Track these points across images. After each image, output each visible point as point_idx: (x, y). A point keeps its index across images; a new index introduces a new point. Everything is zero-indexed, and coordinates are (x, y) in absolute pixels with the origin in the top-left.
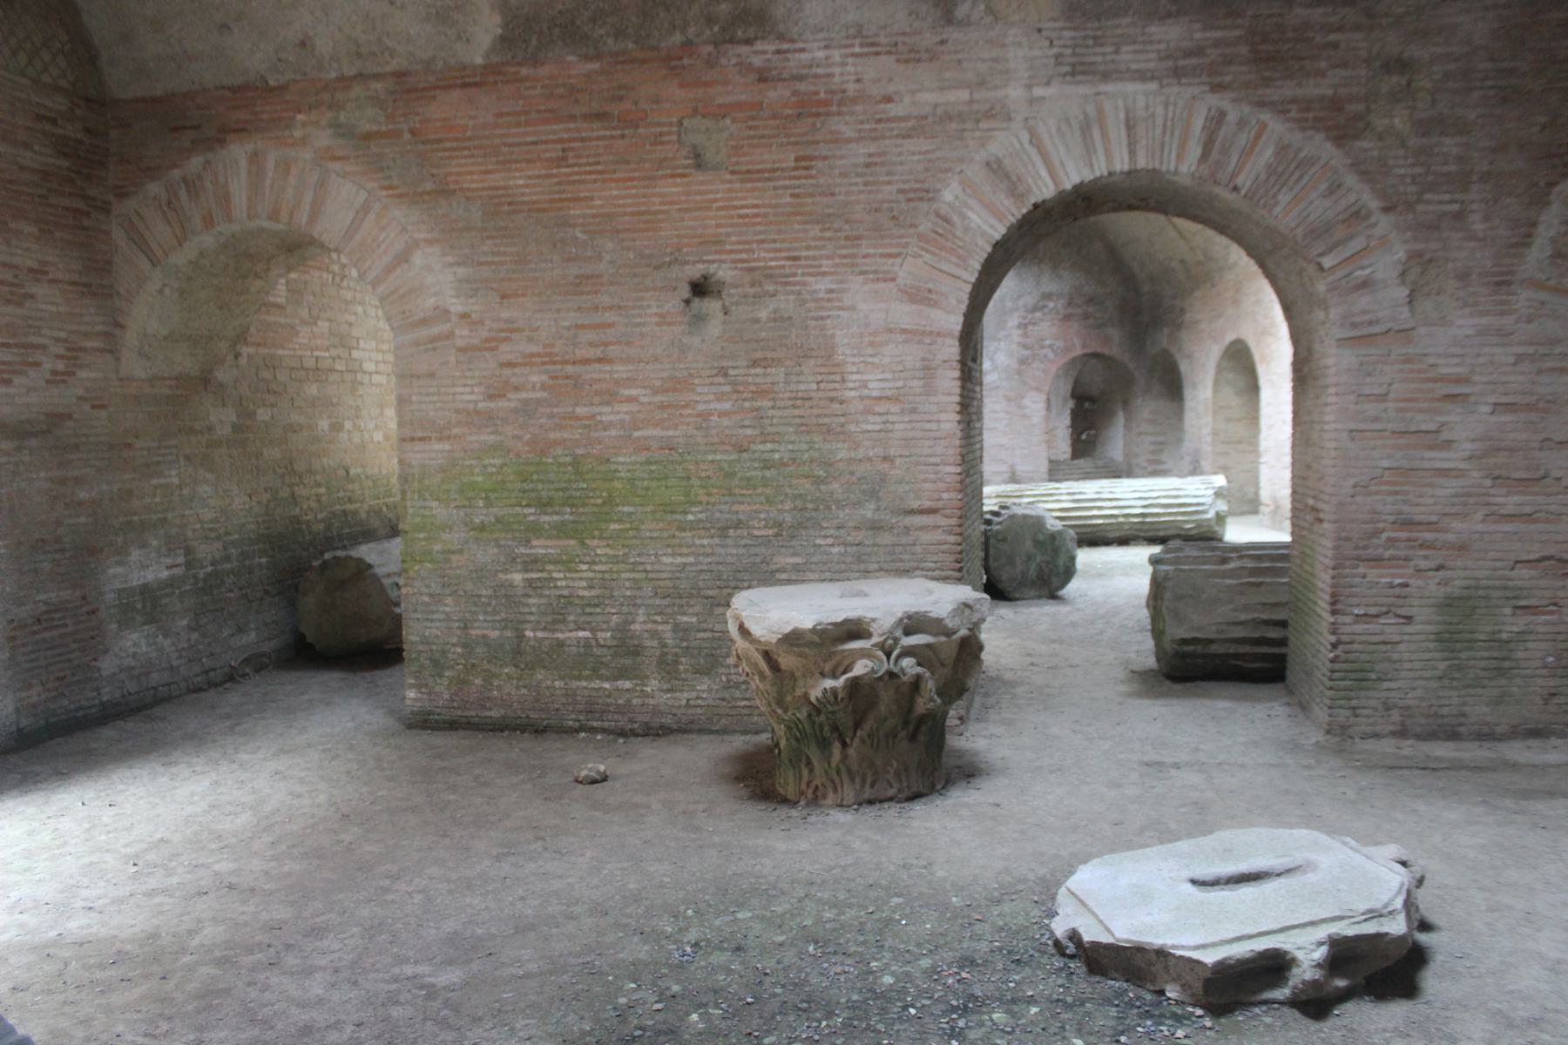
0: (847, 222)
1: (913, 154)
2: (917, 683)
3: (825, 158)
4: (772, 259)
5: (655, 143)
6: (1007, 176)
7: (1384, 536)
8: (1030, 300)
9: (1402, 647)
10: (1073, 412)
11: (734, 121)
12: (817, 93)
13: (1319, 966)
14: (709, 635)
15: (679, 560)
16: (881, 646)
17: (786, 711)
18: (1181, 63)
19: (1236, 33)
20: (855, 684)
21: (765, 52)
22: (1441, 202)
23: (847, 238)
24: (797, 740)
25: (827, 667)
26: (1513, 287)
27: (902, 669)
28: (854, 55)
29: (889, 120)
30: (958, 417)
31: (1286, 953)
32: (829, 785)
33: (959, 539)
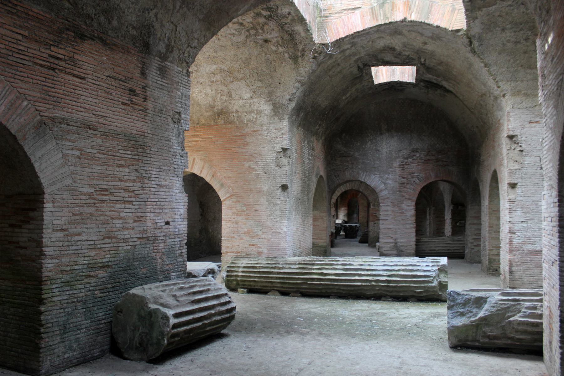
8: (405, 153)
10: (452, 210)
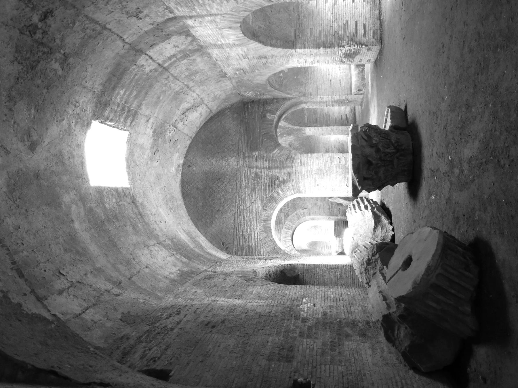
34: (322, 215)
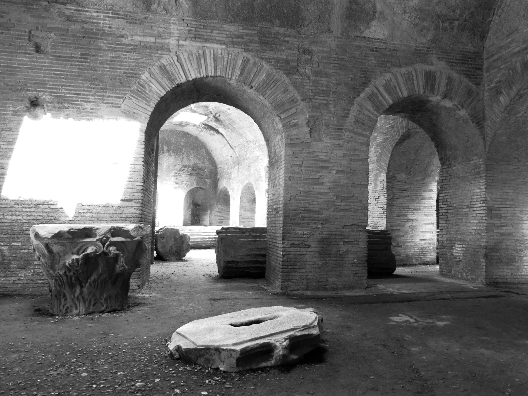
0: (102, 82)
1: (131, 59)
2: (117, 256)
3: (94, 56)
4: (67, 93)
5: (17, 39)
6: (168, 72)
7: (301, 215)
8: (179, 167)
9: (307, 256)
11: (54, 34)
12: (92, 29)
13: (285, 348)
14: (27, 251)
15: (14, 218)
16: (100, 240)
17: (54, 271)
18: (234, 40)
19: (254, 32)
20: (87, 257)
21: (71, 9)
22: (320, 99)
23: (101, 88)
24: (60, 286)
25: (75, 250)
26: (343, 131)
27: (110, 251)
28: (109, 17)
29: (121, 45)
30: (143, 163)
31: (272, 344)
32: (74, 306)
33: (141, 212)
34: (287, 187)
